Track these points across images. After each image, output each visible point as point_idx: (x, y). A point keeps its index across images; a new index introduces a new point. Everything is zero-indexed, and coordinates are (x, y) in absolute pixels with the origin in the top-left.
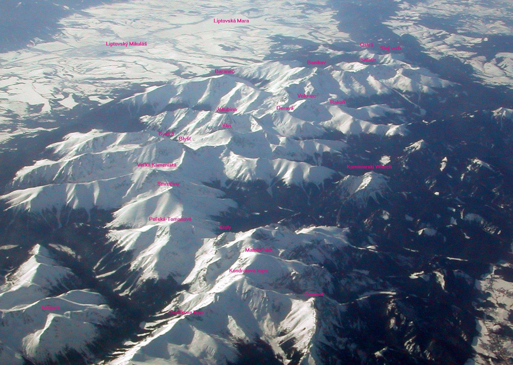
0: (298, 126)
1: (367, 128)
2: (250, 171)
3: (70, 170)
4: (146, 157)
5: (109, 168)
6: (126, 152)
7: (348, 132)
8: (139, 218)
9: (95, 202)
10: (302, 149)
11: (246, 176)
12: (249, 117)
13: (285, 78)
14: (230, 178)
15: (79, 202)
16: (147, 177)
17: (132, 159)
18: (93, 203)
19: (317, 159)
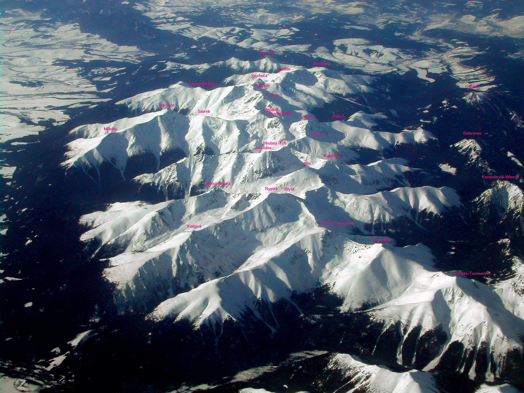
0: (333, 150)
1: (393, 139)
2: (383, 208)
3: (189, 256)
4: (264, 219)
5: (228, 243)
6: (234, 219)
7: (379, 147)
8: (377, 290)
9: (290, 287)
10: (381, 174)
11: (384, 216)
12: (289, 150)
13: (219, 101)
14: (366, 222)
15: (273, 291)
16: (322, 241)
17: (247, 227)
18: (288, 289)
19: (401, 181)
